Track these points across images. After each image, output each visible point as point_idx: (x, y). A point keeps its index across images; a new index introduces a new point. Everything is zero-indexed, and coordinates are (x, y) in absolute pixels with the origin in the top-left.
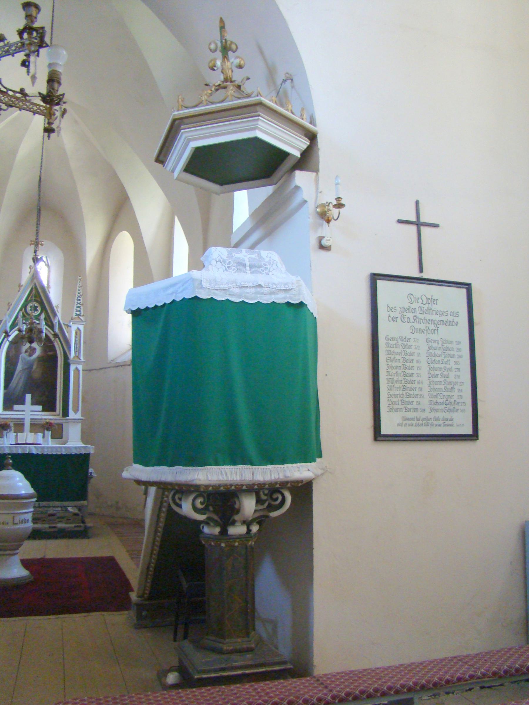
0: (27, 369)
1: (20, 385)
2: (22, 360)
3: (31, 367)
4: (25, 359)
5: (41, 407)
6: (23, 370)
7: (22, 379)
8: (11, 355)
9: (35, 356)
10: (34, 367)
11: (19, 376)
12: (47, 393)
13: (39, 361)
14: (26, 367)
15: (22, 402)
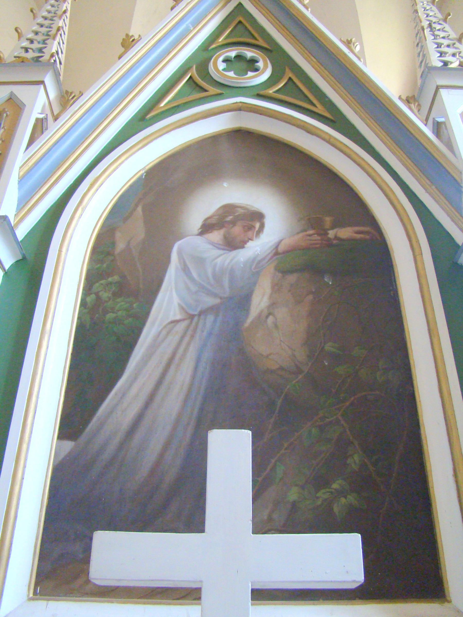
0: (214, 309)
1: (171, 404)
2: (185, 269)
3: (243, 301)
4: (200, 261)
5: (353, 542)
6: (191, 317)
7: (183, 375)
8: (120, 246)
9: (259, 246)
10: (260, 301)
11: (166, 349)
12: (355, 460)
13: (284, 272)
14: (210, 301)
15: (177, 504)
